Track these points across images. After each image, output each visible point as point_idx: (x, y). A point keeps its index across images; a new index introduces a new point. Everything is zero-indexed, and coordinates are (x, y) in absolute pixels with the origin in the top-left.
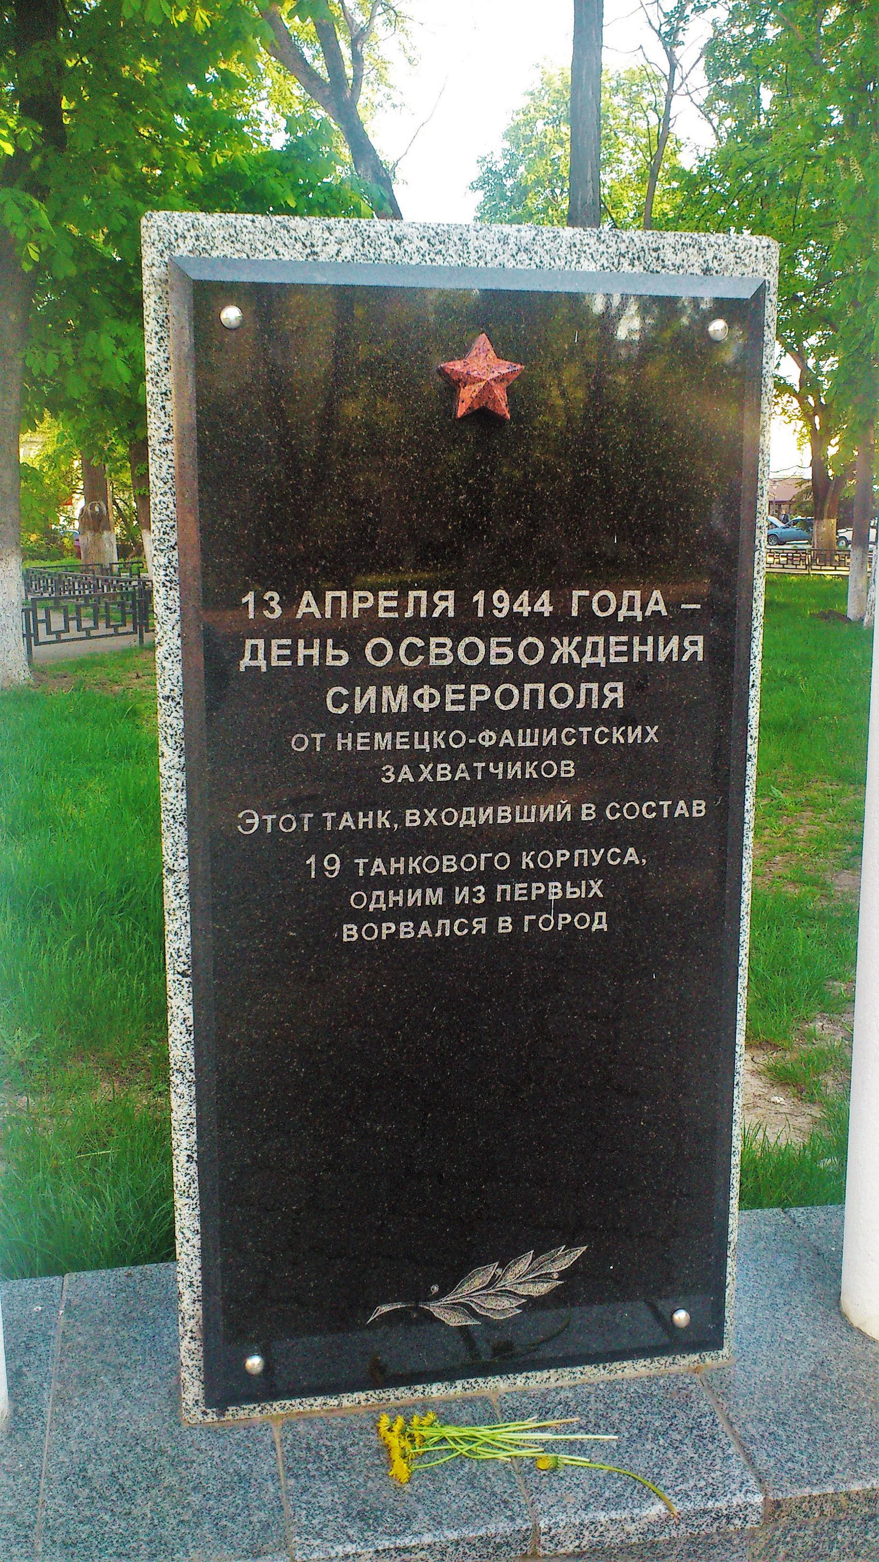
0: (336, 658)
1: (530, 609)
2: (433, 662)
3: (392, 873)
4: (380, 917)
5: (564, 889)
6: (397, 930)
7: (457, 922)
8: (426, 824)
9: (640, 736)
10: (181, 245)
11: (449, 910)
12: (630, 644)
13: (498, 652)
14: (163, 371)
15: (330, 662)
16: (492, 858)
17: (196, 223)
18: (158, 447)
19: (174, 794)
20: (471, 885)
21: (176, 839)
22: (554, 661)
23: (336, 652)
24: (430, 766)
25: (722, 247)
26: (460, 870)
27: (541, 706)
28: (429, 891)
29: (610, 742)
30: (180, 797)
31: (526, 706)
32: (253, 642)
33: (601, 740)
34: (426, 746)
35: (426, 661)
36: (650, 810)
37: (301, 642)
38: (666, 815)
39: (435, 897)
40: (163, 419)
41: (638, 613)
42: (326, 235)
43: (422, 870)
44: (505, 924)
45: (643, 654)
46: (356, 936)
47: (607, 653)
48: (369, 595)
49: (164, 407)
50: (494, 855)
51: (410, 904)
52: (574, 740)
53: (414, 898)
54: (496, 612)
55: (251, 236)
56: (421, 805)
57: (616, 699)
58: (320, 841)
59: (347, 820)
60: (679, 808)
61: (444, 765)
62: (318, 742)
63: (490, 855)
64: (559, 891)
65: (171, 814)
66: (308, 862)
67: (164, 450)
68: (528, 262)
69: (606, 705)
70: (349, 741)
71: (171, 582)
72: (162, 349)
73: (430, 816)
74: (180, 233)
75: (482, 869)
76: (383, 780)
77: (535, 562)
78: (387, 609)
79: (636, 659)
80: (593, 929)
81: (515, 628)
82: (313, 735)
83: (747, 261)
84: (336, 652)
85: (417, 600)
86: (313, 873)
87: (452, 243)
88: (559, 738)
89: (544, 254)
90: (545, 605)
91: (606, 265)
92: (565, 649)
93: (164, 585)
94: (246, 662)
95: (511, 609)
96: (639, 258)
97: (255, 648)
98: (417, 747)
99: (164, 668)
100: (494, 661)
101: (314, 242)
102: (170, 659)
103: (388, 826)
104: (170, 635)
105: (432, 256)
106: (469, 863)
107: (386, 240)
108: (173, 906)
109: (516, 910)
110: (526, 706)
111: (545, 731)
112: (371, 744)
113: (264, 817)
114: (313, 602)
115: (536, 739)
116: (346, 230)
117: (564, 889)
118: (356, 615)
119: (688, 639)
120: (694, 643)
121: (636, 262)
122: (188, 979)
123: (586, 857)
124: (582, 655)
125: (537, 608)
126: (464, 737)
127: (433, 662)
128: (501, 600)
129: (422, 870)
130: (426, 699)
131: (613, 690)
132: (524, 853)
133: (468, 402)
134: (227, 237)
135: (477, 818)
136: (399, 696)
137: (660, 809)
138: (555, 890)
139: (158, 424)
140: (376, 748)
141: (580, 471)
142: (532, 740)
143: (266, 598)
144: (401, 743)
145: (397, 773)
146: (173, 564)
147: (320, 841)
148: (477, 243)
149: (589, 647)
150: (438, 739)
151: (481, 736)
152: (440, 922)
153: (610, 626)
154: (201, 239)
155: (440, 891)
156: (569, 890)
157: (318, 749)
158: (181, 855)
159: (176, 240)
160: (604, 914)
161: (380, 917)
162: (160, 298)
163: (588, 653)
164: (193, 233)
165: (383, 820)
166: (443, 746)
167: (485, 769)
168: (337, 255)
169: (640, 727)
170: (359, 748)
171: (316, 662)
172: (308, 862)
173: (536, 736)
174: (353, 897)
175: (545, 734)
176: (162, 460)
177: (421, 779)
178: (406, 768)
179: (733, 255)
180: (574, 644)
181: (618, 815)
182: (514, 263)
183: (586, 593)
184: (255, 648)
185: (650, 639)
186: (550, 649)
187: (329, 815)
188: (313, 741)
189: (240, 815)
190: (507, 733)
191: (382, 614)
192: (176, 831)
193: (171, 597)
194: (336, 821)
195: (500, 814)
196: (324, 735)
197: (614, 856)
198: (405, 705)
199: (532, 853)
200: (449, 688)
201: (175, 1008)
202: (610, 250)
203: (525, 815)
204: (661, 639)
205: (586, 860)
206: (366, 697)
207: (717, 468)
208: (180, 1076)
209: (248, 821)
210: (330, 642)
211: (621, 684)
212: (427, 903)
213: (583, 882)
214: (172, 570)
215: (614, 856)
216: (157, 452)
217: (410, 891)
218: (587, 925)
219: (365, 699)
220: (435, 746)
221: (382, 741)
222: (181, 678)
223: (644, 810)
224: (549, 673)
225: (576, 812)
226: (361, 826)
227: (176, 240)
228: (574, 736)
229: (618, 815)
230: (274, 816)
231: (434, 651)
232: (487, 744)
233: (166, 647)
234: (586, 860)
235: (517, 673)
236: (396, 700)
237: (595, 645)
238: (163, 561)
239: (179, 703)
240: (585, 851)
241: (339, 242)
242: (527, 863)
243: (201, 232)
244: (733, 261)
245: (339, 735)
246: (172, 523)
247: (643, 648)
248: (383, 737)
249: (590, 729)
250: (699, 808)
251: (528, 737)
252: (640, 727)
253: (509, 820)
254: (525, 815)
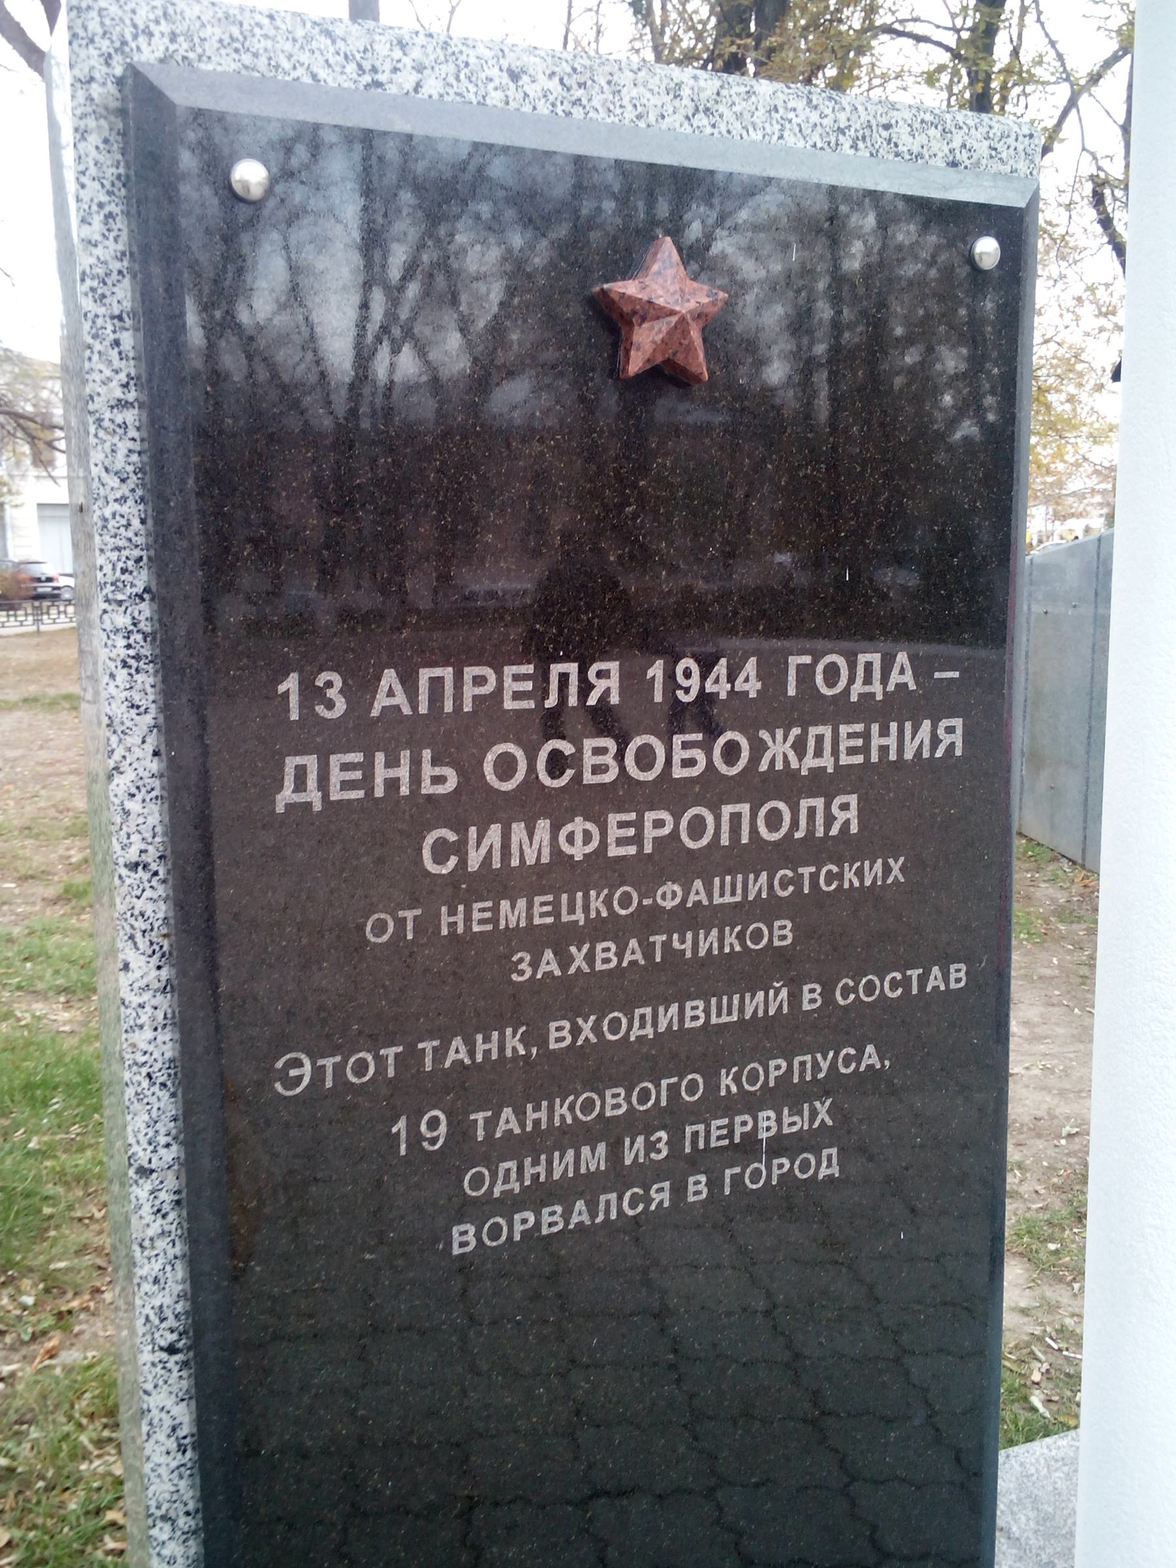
0: (438, 780)
1: (729, 686)
2: (588, 778)
3: (529, 1129)
4: (510, 1205)
5: (779, 1121)
6: (538, 1224)
7: (628, 1194)
8: (580, 1043)
9: (880, 874)
10: (144, 47)
11: (618, 1176)
12: (866, 735)
13: (686, 756)
14: (115, 276)
15: (427, 788)
16: (678, 1085)
17: (171, 10)
18: (107, 415)
19: (148, 1034)
20: (649, 1131)
21: (154, 1113)
22: (764, 766)
23: (438, 771)
24: (586, 948)
25: (973, 131)
26: (631, 1110)
27: (745, 840)
28: (586, 1151)
29: (840, 886)
30: (160, 1039)
31: (725, 841)
32: (299, 760)
33: (828, 884)
34: (579, 917)
35: (578, 776)
36: (894, 985)
37: (380, 758)
38: (915, 991)
39: (594, 1158)
40: (117, 363)
41: (877, 688)
42: (397, 53)
43: (575, 1118)
44: (698, 1187)
45: (884, 750)
46: (473, 1243)
47: (835, 752)
48: (488, 672)
49: (117, 343)
50: (681, 1080)
51: (556, 1176)
52: (791, 888)
53: (562, 1165)
54: (680, 694)
55: (269, 44)
56: (573, 1012)
57: (847, 823)
59: (457, 1051)
60: (932, 977)
61: (605, 944)
62: (410, 926)
63: (674, 1080)
64: (773, 1123)
65: (144, 1071)
66: (394, 1130)
67: (119, 420)
68: (709, 130)
69: (834, 831)
70: (460, 918)
71: (137, 658)
72: (112, 235)
73: (586, 1027)
74: (141, 26)
75: (664, 1103)
76: (515, 977)
77: (735, 613)
78: (517, 696)
79: (875, 758)
80: (821, 1177)
81: (704, 716)
82: (401, 914)
83: (1004, 155)
84: (438, 771)
85: (564, 678)
86: (403, 1147)
87: (597, 87)
88: (771, 886)
89: (732, 119)
90: (750, 683)
91: (819, 145)
92: (779, 748)
93: (125, 664)
94: (287, 795)
95: (702, 688)
96: (864, 138)
97: (301, 773)
98: (565, 918)
99: (127, 813)
100: (678, 773)
101: (378, 64)
102: (139, 797)
103: (522, 1052)
104: (138, 753)
105: (567, 106)
106: (644, 1096)
107: (494, 72)
108: (150, 1232)
109: (704, 1160)
110: (725, 841)
111: (752, 876)
112: (495, 921)
113: (320, 1062)
114: (398, 688)
115: (739, 891)
116: (430, 49)
117: (779, 1121)
118: (468, 707)
119: (944, 723)
120: (950, 730)
121: (861, 145)
122: (178, 1357)
123: (809, 1066)
124: (801, 755)
125: (739, 685)
126: (635, 896)
127: (588, 778)
128: (687, 674)
129: (575, 1118)
130: (578, 839)
131: (845, 807)
132: (723, 1071)
133: (648, 348)
134: (227, 40)
135: (655, 1024)
136: (536, 838)
137: (907, 981)
138: (767, 1123)
139: (108, 373)
140: (502, 926)
141: (800, 467)
142: (733, 893)
143: (320, 683)
144: (542, 915)
145: (535, 965)
146: (142, 626)
147: (412, 1090)
148: (634, 93)
149: (811, 743)
150: (597, 904)
151: (659, 892)
152: (603, 1198)
154: (181, 39)
155: (602, 1148)
156: (786, 1120)
157: (410, 937)
158: (163, 1140)
159: (135, 37)
160: (834, 1151)
161: (510, 1205)
162: (106, 141)
163: (811, 750)
164: (164, 27)
165: (514, 1043)
166: (604, 914)
167: (667, 945)
168: (416, 90)
169: (880, 861)
170: (476, 928)
171: (404, 790)
172: (394, 1130)
173: (739, 885)
174: (467, 1178)
175: (751, 882)
176: (116, 439)
177: (572, 970)
178: (549, 955)
179: (986, 143)
180: (791, 739)
181: (852, 996)
182: (689, 130)
183: (807, 659)
184: (301, 773)
185: (894, 726)
186: (758, 748)
187: (427, 1046)
188: (401, 923)
189: (279, 1064)
190: (698, 884)
191: (509, 704)
192: (153, 1100)
193: (139, 686)
194: (440, 1054)
195: (689, 1013)
196: (418, 912)
197: (847, 1061)
198: (546, 852)
199: (735, 1069)
200: (613, 819)
201: (155, 1412)
202: (825, 122)
203: (725, 1010)
204: (908, 725)
205: (809, 1072)
206: (486, 843)
207: (982, 465)
208: (167, 1527)
209: (293, 1073)
210: (427, 754)
211: (855, 796)
212: (583, 1170)
213: (806, 1106)
214: (139, 637)
215: (847, 1061)
216: (106, 424)
217: (557, 1154)
218: (812, 1171)
219: (484, 848)
220: (593, 915)
221: (512, 914)
222: (159, 829)
223: (887, 987)
224: (760, 786)
225: (795, 998)
226: (479, 1058)
227: (135, 37)
228: (791, 881)
229: (852, 996)
230: (338, 1059)
231: (589, 760)
232: (669, 904)
233: (130, 775)
234: (809, 1072)
235: (712, 789)
236: (532, 844)
237: (820, 739)
238: (123, 620)
239: (156, 874)
240: (808, 1058)
241: (419, 68)
242: (728, 1087)
243: (180, 28)
244: (986, 152)
245: (444, 909)
246: (137, 553)
247: (884, 741)
248: (513, 907)
249: (813, 869)
250: (959, 974)
251: (728, 888)
252: (880, 861)
253: (702, 1021)
254: (725, 1010)
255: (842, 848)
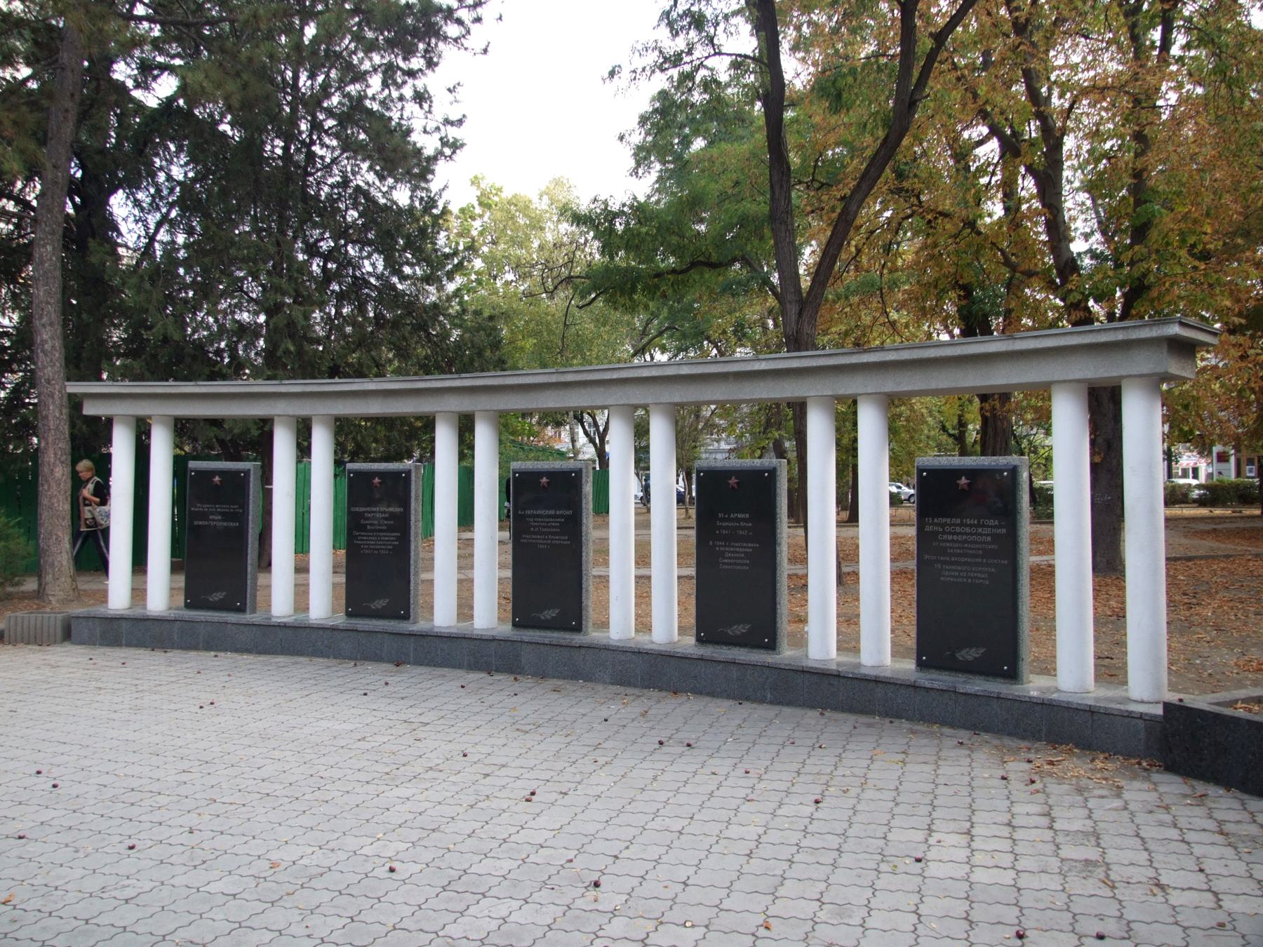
13: (968, 530)
58: (938, 561)
81: (971, 526)
130: (955, 537)
224: (976, 534)
235: (971, 534)
255: (989, 543)
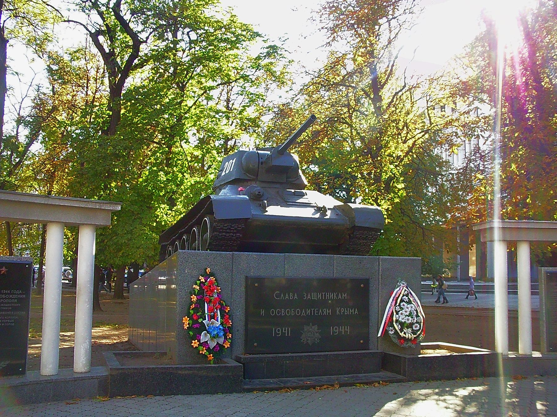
44: (3, 324)
92: (11, 296)
153: (16, 294)
224: (9, 298)
235: (6, 298)
